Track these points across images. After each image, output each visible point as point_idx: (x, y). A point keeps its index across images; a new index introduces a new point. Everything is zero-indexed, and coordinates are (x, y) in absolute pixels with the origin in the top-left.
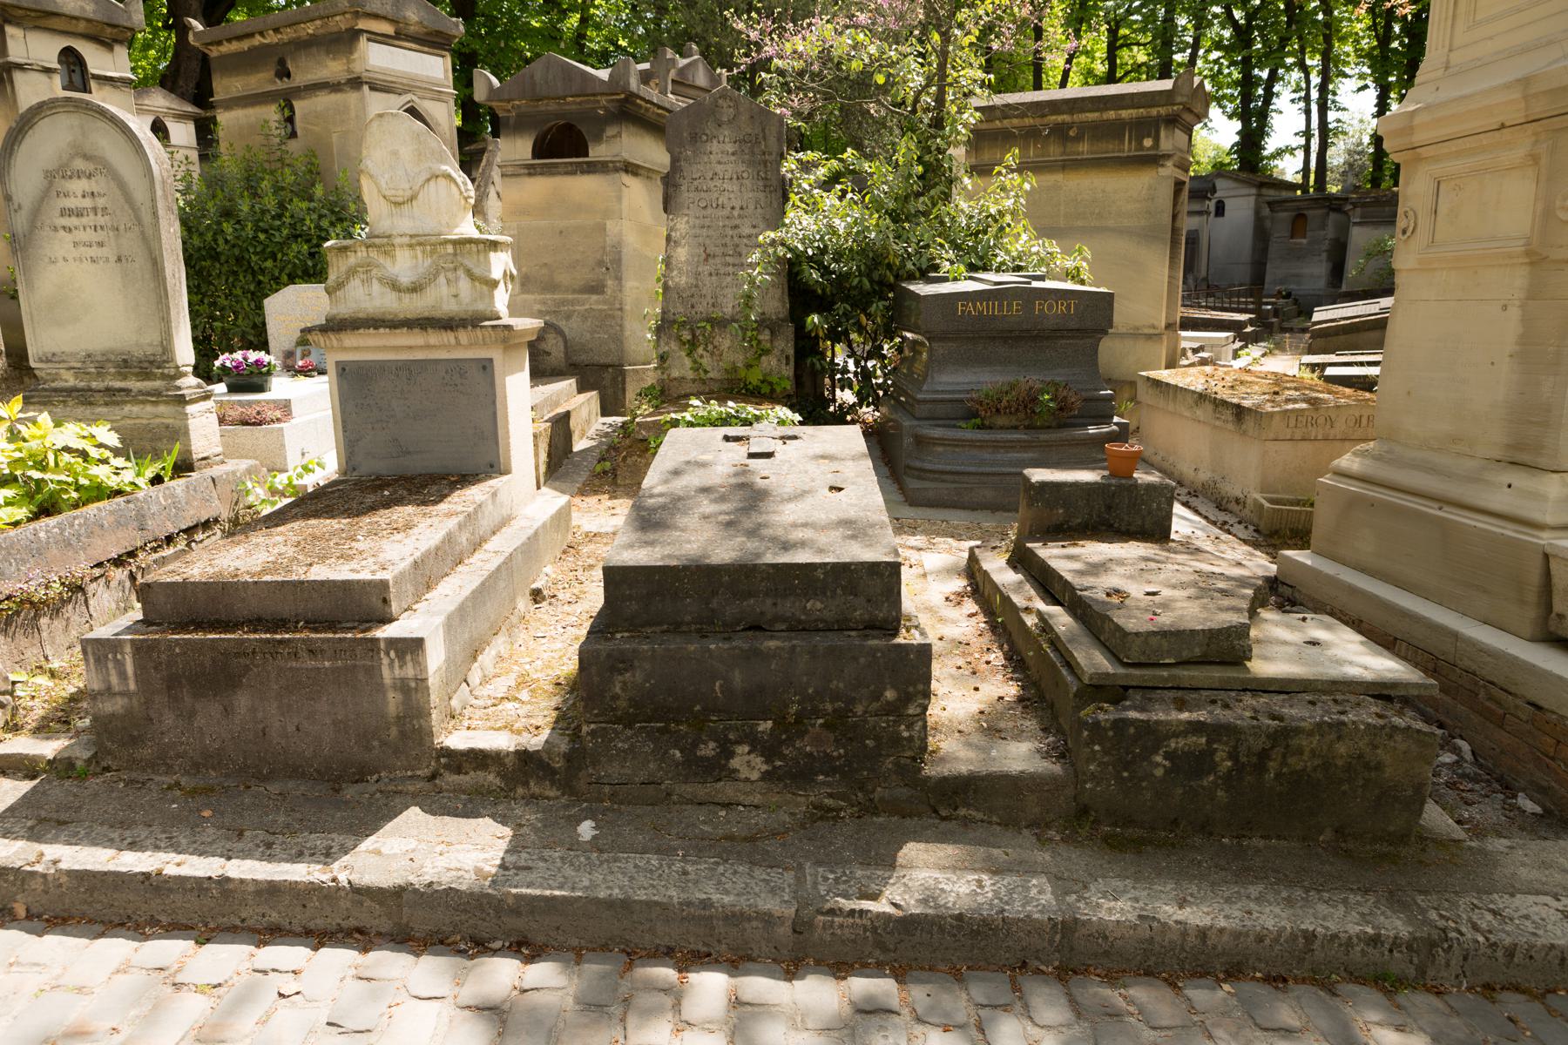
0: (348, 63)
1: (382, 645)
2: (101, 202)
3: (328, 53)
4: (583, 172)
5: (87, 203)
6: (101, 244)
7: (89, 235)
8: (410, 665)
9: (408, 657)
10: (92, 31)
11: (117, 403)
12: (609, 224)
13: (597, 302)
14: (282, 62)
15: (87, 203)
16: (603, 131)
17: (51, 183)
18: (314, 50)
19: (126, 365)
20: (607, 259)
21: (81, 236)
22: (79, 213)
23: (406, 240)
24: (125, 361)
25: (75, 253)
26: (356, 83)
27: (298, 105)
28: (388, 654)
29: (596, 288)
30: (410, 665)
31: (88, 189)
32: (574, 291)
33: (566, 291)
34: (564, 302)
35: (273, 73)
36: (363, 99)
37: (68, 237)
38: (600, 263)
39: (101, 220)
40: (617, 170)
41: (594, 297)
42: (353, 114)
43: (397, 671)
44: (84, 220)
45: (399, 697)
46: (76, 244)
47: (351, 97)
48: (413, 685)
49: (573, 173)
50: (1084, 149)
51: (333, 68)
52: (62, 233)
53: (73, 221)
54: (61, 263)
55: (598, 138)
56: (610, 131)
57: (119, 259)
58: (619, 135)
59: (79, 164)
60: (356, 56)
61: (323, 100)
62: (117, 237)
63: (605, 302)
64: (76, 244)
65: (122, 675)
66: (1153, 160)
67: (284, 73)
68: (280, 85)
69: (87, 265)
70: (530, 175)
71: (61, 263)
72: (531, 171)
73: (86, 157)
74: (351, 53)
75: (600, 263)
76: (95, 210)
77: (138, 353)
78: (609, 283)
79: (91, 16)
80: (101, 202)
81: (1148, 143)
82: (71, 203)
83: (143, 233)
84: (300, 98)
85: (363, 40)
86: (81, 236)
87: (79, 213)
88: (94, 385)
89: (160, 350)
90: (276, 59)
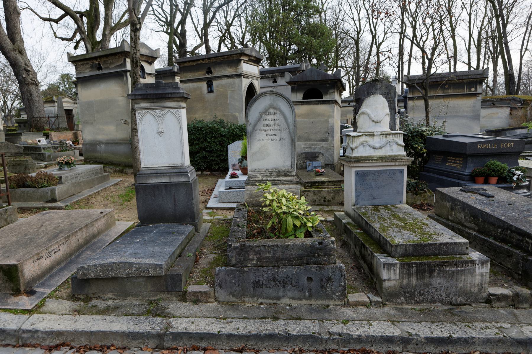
0: (236, 69)
1: (477, 262)
2: (277, 122)
3: (228, 66)
4: (321, 104)
5: (273, 122)
6: (275, 135)
7: (272, 132)
8: (485, 268)
9: (485, 265)
10: (147, 60)
11: (276, 185)
12: (330, 120)
13: (325, 144)
14: (209, 68)
15: (273, 122)
16: (329, 91)
17: (261, 116)
18: (223, 65)
19: (279, 173)
20: (329, 131)
21: (269, 132)
22: (269, 125)
23: (379, 133)
24: (279, 171)
25: (267, 138)
26: (239, 76)
27: (215, 83)
28: (478, 264)
29: (325, 140)
30: (485, 268)
31: (273, 118)
32: (317, 141)
33: (314, 141)
34: (313, 145)
35: (205, 72)
36: (241, 80)
37: (265, 133)
38: (326, 132)
39: (276, 127)
40: (333, 103)
41: (324, 143)
42: (237, 85)
43: (480, 270)
44: (271, 128)
45: (480, 278)
46: (267, 135)
47: (237, 80)
48: (484, 274)
49: (318, 104)
50: (451, 92)
51: (230, 71)
52: (263, 131)
53: (267, 128)
54: (261, 141)
55: (327, 93)
56: (331, 91)
57: (281, 140)
58: (334, 92)
59: (271, 110)
60: (239, 67)
61: (225, 81)
62: (281, 133)
63: (328, 144)
64: (267, 135)
65: (395, 274)
66: (475, 95)
67: (209, 72)
68: (207, 76)
69: (270, 141)
70: (302, 104)
71: (261, 141)
72: (302, 103)
73: (274, 108)
74: (238, 66)
75: (326, 132)
76: (275, 124)
77: (283, 169)
78: (329, 138)
79: (148, 54)
80: (277, 122)
81: (473, 89)
82: (267, 122)
83: (289, 131)
84: (216, 80)
85: (242, 62)
86: (269, 132)
87: (269, 125)
88: (269, 179)
89: (290, 167)
90: (207, 68)
